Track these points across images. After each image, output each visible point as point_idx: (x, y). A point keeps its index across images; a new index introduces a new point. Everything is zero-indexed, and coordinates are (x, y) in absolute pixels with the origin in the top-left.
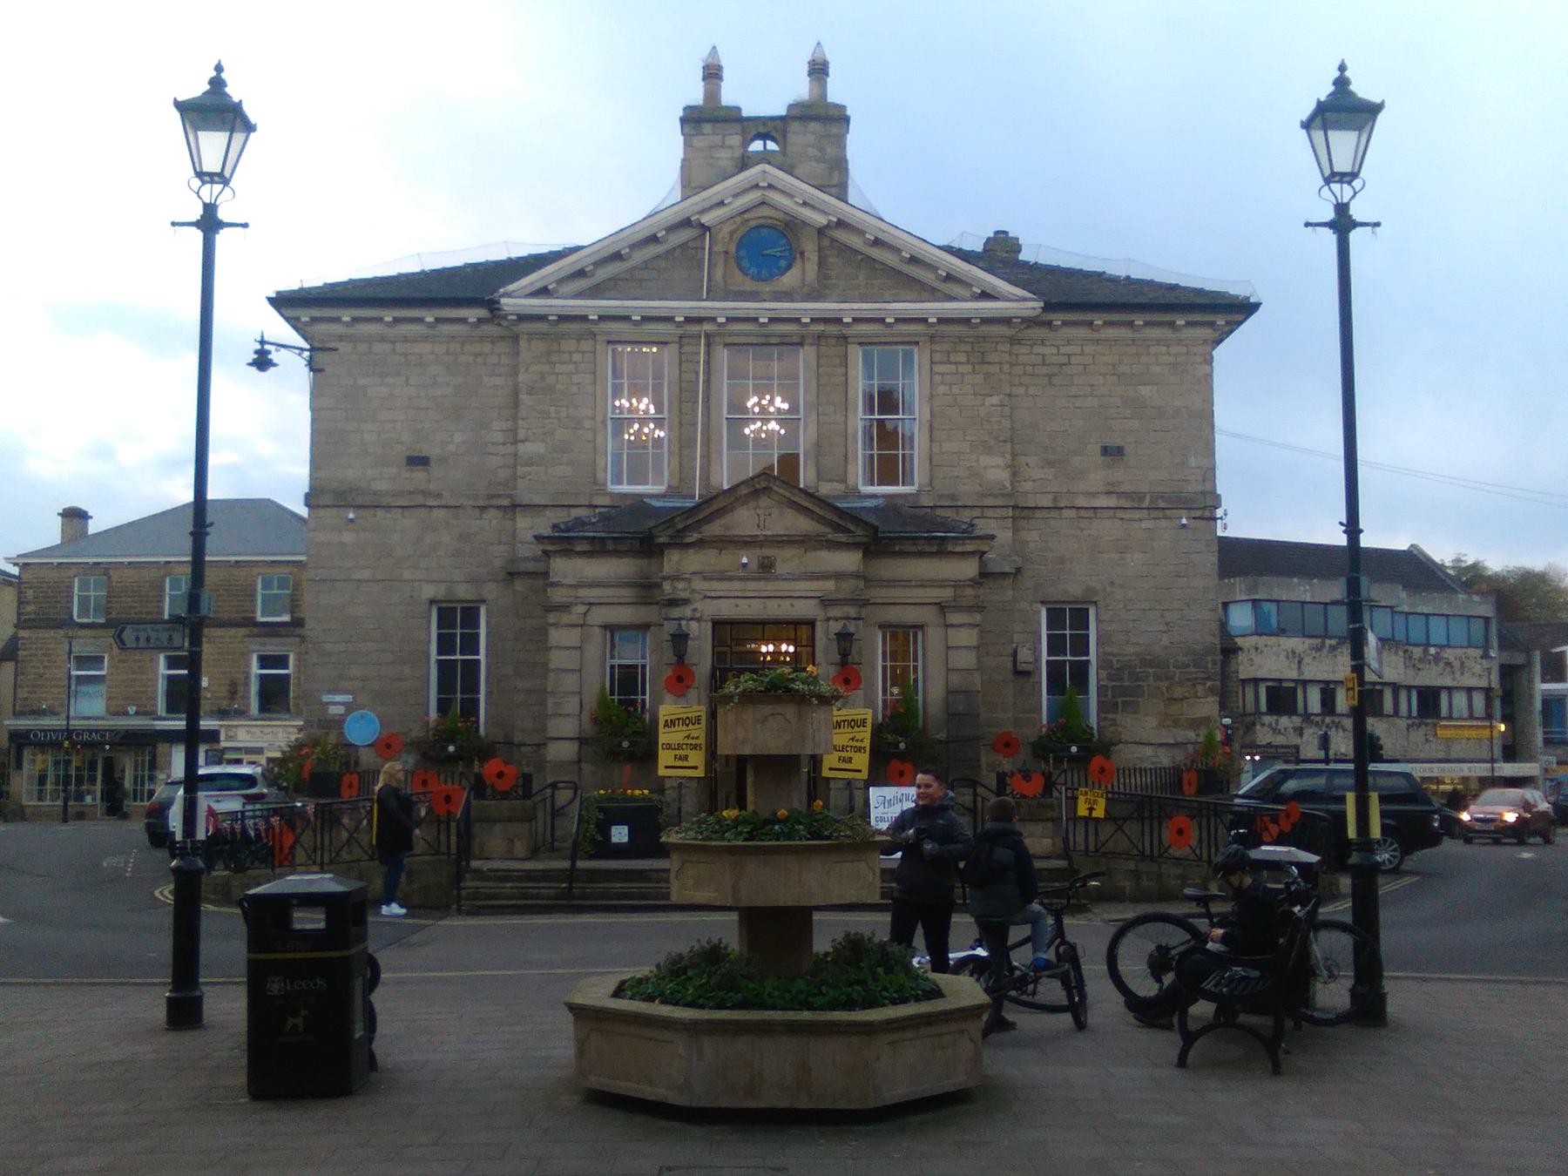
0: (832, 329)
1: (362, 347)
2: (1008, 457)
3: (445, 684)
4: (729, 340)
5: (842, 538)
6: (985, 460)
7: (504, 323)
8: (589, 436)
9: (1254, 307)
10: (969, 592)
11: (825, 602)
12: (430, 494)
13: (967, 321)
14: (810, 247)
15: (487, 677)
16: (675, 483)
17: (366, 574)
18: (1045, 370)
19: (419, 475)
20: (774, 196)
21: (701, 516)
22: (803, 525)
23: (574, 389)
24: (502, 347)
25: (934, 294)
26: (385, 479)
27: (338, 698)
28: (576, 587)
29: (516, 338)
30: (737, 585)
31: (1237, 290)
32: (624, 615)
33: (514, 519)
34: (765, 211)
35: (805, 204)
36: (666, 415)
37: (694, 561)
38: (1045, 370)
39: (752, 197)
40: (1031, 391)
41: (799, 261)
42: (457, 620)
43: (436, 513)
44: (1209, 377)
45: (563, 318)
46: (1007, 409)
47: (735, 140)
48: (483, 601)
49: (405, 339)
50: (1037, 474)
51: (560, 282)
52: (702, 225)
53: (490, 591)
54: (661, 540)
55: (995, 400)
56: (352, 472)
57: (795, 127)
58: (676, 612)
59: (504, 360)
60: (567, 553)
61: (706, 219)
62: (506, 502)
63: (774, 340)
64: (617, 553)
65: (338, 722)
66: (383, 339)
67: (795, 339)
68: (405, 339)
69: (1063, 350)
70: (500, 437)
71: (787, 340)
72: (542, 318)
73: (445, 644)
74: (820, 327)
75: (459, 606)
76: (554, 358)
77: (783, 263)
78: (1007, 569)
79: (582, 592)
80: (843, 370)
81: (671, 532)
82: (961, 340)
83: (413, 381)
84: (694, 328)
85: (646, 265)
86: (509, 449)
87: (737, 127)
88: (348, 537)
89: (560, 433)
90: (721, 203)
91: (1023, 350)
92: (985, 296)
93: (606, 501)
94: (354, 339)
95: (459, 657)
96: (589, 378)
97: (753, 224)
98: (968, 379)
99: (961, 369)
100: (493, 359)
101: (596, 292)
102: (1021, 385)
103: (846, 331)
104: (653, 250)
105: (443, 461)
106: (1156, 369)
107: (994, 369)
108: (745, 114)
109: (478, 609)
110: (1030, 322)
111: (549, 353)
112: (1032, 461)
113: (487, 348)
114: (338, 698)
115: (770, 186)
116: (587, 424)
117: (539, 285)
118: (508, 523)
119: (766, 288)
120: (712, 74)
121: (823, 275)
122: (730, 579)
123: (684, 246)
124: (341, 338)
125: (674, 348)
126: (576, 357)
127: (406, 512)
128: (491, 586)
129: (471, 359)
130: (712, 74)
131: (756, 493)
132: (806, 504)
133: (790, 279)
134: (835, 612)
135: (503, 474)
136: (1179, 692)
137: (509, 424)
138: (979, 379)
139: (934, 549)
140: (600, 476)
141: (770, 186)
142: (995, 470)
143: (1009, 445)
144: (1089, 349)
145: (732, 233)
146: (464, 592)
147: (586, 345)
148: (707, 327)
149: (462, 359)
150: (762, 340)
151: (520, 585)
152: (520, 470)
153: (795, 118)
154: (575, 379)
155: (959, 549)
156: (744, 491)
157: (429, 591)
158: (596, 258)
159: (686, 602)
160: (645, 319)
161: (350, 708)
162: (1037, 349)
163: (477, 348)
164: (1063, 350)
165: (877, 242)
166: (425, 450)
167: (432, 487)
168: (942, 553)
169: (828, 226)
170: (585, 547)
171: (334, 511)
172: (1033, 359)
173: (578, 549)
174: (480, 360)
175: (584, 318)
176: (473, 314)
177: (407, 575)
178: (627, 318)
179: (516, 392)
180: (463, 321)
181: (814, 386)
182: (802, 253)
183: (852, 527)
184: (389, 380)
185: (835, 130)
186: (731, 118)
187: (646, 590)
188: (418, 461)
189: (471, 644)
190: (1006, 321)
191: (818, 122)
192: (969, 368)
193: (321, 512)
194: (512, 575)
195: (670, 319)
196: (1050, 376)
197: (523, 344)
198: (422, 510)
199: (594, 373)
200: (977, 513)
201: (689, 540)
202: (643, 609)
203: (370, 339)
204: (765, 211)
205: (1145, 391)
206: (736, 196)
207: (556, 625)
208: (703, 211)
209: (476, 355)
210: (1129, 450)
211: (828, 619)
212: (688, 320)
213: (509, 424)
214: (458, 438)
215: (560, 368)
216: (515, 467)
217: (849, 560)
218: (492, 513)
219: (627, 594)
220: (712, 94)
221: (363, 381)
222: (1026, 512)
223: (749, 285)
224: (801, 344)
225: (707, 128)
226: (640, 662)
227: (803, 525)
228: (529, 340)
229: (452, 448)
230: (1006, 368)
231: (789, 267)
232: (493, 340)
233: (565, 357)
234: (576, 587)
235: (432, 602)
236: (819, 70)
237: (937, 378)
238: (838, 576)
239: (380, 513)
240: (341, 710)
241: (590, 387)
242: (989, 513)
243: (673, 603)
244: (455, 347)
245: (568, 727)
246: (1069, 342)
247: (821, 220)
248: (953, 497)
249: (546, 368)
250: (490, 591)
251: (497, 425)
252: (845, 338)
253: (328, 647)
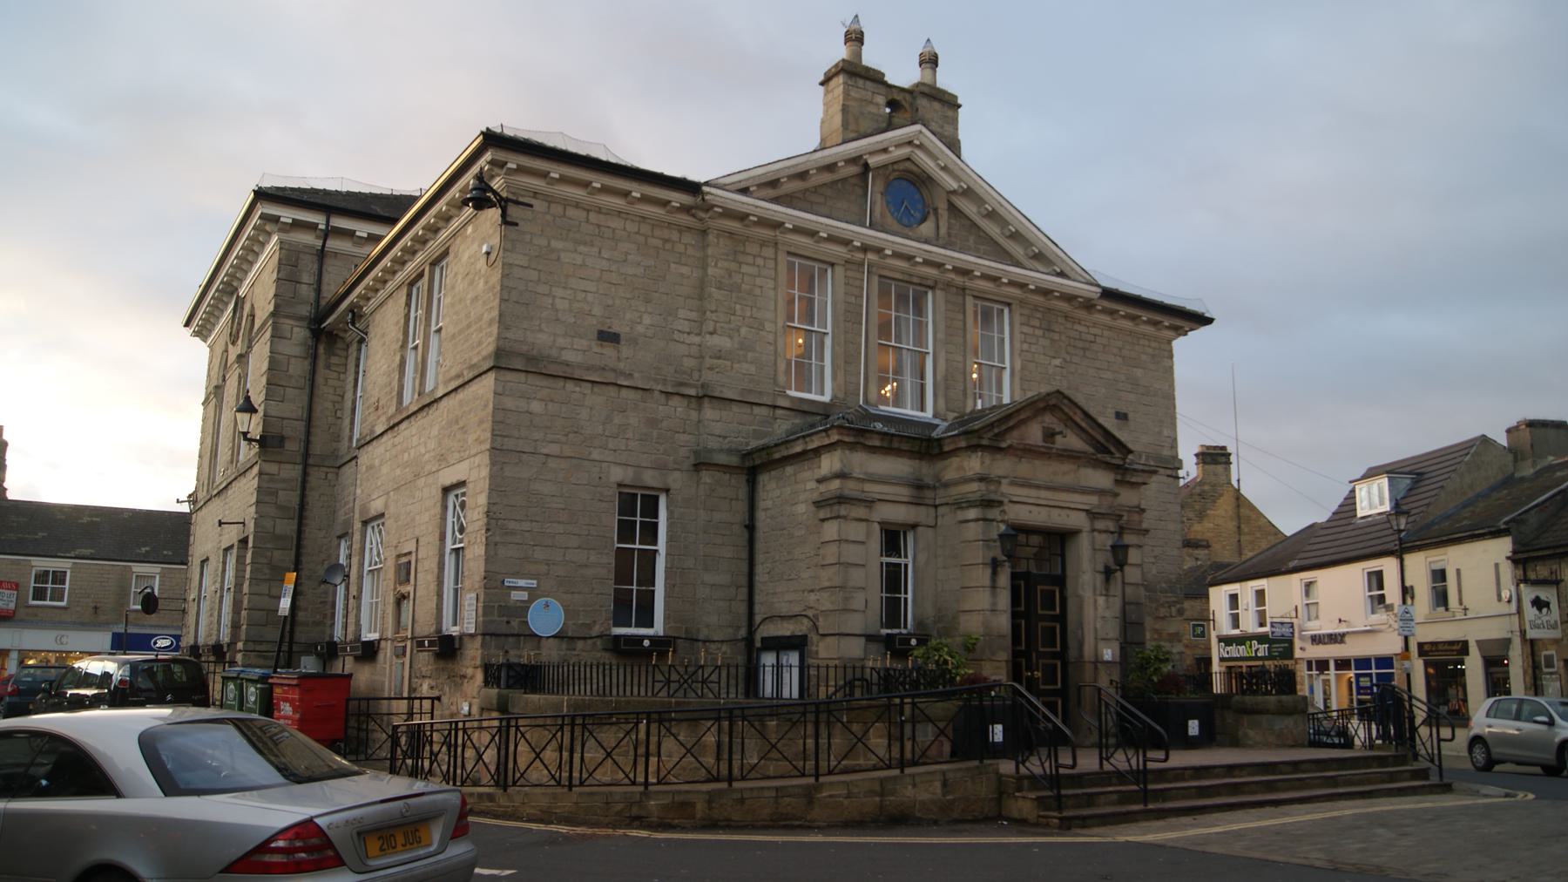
0: (959, 280)
1: (557, 209)
3: (622, 575)
5: (1107, 458)
7: (702, 215)
8: (771, 338)
9: (1209, 321)
10: (1136, 517)
11: (1092, 515)
12: (622, 373)
13: (1045, 292)
15: (668, 570)
16: (841, 395)
17: (553, 449)
19: (609, 351)
20: (921, 156)
21: (1011, 423)
22: (1072, 441)
23: (757, 291)
24: (688, 238)
25: (1018, 264)
26: (577, 352)
27: (522, 583)
28: (863, 480)
29: (704, 232)
30: (1033, 492)
31: (1192, 306)
32: (898, 514)
33: (700, 410)
34: (908, 165)
35: (944, 169)
36: (829, 330)
37: (1002, 466)
38: (1080, 344)
39: (906, 151)
40: (1076, 359)
41: (932, 219)
42: (637, 509)
43: (624, 392)
44: (1172, 368)
45: (764, 222)
47: (881, 100)
48: (667, 491)
49: (599, 211)
51: (760, 186)
52: (866, 165)
53: (676, 480)
54: (985, 442)
55: (1057, 362)
56: (543, 339)
57: (923, 102)
58: (994, 513)
59: (690, 251)
60: (852, 446)
61: (873, 161)
62: (692, 392)
63: (915, 280)
64: (898, 452)
65: (523, 609)
66: (577, 206)
67: (930, 283)
68: (599, 211)
69: (1093, 330)
70: (686, 326)
72: (742, 217)
73: (626, 531)
74: (952, 276)
75: (639, 492)
76: (741, 258)
77: (918, 215)
79: (868, 487)
80: (960, 317)
81: (990, 435)
82: (1036, 308)
83: (605, 254)
84: (860, 256)
85: (816, 190)
86: (697, 340)
87: (883, 89)
88: (536, 406)
89: (743, 331)
90: (885, 150)
91: (1069, 325)
92: (1062, 274)
93: (786, 404)
94: (550, 200)
95: (637, 546)
96: (771, 284)
98: (1042, 341)
100: (680, 248)
101: (775, 200)
103: (968, 284)
104: (827, 177)
105: (634, 341)
106: (1144, 357)
107: (1056, 337)
108: (890, 79)
109: (656, 499)
110: (1088, 305)
111: (736, 252)
113: (675, 236)
114: (522, 583)
115: (921, 146)
116: (769, 326)
117: (743, 185)
118: (694, 415)
119: (906, 231)
120: (855, 38)
121: (949, 235)
122: (1031, 486)
123: (844, 180)
124: (535, 194)
125: (839, 270)
126: (760, 261)
127: (596, 389)
128: (677, 474)
129: (659, 243)
130: (855, 38)
131: (1044, 409)
132: (1083, 424)
133: (927, 228)
134: (1100, 525)
135: (689, 363)
136: (1163, 612)
137: (694, 315)
138: (1047, 343)
140: (782, 379)
141: (921, 146)
144: (1106, 333)
146: (650, 479)
147: (769, 252)
148: (871, 256)
149: (652, 241)
150: (906, 278)
151: (707, 477)
152: (708, 362)
153: (923, 94)
154: (758, 281)
156: (1042, 405)
157: (618, 474)
158: (792, 171)
159: (1001, 503)
160: (832, 239)
161: (534, 594)
162: (1077, 327)
163: (666, 233)
164: (1093, 330)
165: (993, 215)
166: (615, 329)
167: (622, 366)
169: (954, 192)
170: (877, 443)
171: (523, 375)
172: (1072, 333)
173: (870, 443)
174: (668, 246)
175: (778, 225)
176: (678, 198)
177: (596, 455)
178: (812, 234)
179: (702, 285)
180: (665, 204)
181: (942, 327)
182: (936, 210)
183: (1113, 449)
184: (582, 248)
185: (950, 113)
186: (875, 78)
187: (919, 489)
188: (608, 337)
189: (651, 532)
190: (1069, 298)
191: (931, 104)
192: (1039, 332)
193: (510, 376)
194: (698, 466)
195: (847, 243)
196: (1084, 349)
197: (711, 238)
198: (611, 388)
199: (775, 279)
201: (1004, 445)
202: (912, 509)
203: (566, 203)
204: (908, 165)
205: (1139, 372)
206: (898, 146)
207: (844, 517)
209: (666, 241)
210: (1131, 416)
211: (1093, 530)
212: (865, 249)
213: (694, 315)
214: (647, 320)
215: (745, 269)
216: (702, 357)
217: (1101, 479)
218: (675, 401)
219: (904, 492)
220: (859, 55)
221: (554, 244)
223: (896, 226)
224: (932, 288)
225: (860, 82)
226: (902, 561)
227: (1072, 441)
228: (718, 237)
229: (640, 329)
231: (924, 220)
232: (683, 229)
233: (750, 259)
234: (863, 480)
235: (620, 485)
236: (930, 61)
238: (1101, 492)
239: (570, 385)
240: (524, 596)
241: (772, 293)
243: (988, 503)
244: (645, 229)
245: (855, 623)
246: (1095, 325)
247: (954, 185)
249: (733, 266)
250: (676, 480)
251: (682, 313)
252: (964, 289)
253: (512, 525)
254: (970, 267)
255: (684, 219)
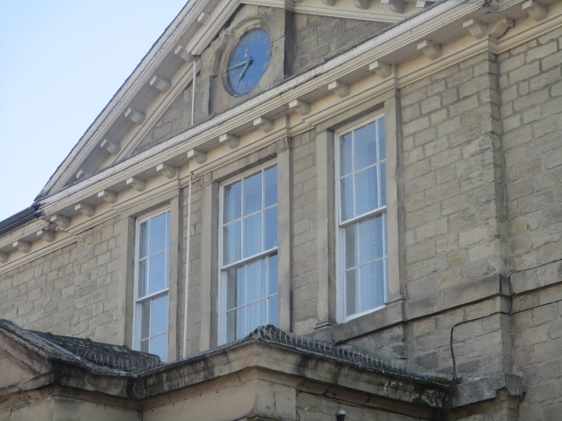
2: (493, 222)
4: (216, 176)
6: (466, 238)
14: (278, 32)
18: (542, 81)
34: (246, 13)
40: (529, 116)
46: (489, 155)
50: (538, 238)
55: (473, 147)
63: (253, 159)
67: (270, 151)
71: (264, 155)
78: (488, 394)
82: (432, 80)
91: (516, 62)
97: (240, 32)
99: (435, 118)
102: (515, 113)
107: (471, 103)
112: (532, 220)
139: (201, 377)
142: (480, 248)
143: (492, 208)
145: (220, 53)
148: (194, 166)
150: (242, 164)
155: (226, 371)
168: (210, 382)
172: (528, 71)
196: (548, 86)
200: (458, 317)
208: (184, 40)
209: (59, 269)
215: (102, 260)
222: (530, 300)
230: (486, 97)
233: (104, 247)
237: (408, 143)
242: (473, 312)
248: (427, 302)
254: (277, 104)
255: (62, 239)
